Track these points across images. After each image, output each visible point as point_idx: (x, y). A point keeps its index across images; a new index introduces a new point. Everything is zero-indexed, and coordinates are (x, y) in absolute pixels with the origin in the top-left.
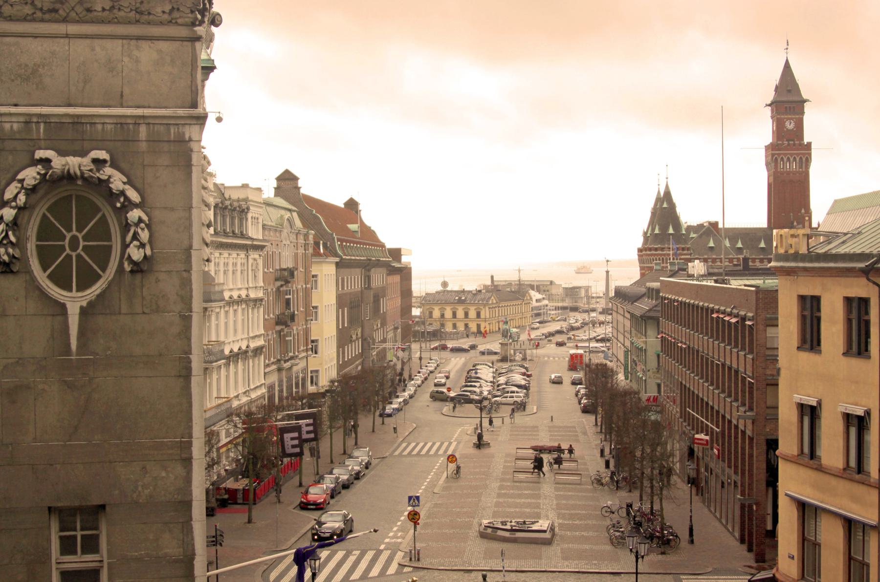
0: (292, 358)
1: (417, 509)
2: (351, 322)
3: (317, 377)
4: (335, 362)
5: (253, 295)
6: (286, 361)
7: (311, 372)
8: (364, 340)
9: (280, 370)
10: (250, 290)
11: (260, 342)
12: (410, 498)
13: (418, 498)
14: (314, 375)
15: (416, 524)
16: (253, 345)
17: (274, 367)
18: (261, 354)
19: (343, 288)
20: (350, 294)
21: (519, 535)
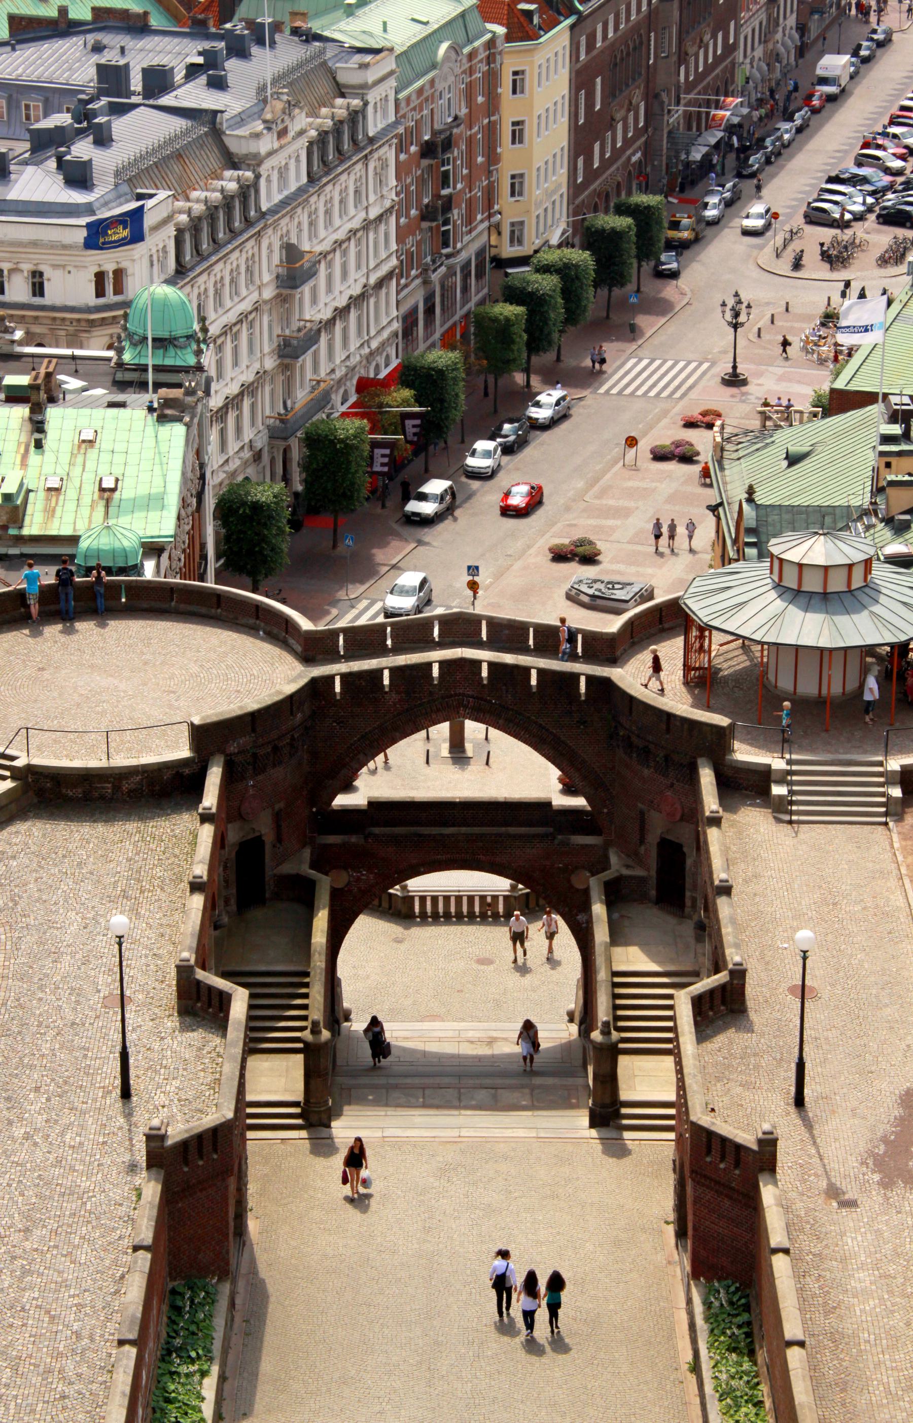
0: (448, 256)
1: (476, 579)
2: (610, 93)
3: (521, 231)
4: (564, 190)
5: (374, 213)
6: (435, 271)
7: (512, 224)
8: (652, 97)
9: (426, 282)
10: (370, 209)
11: (394, 262)
12: (469, 568)
13: (477, 568)
14: (516, 228)
15: (475, 593)
16: (372, 280)
17: (418, 281)
18: (391, 278)
19: (591, 45)
20: (612, 44)
21: (599, 602)
